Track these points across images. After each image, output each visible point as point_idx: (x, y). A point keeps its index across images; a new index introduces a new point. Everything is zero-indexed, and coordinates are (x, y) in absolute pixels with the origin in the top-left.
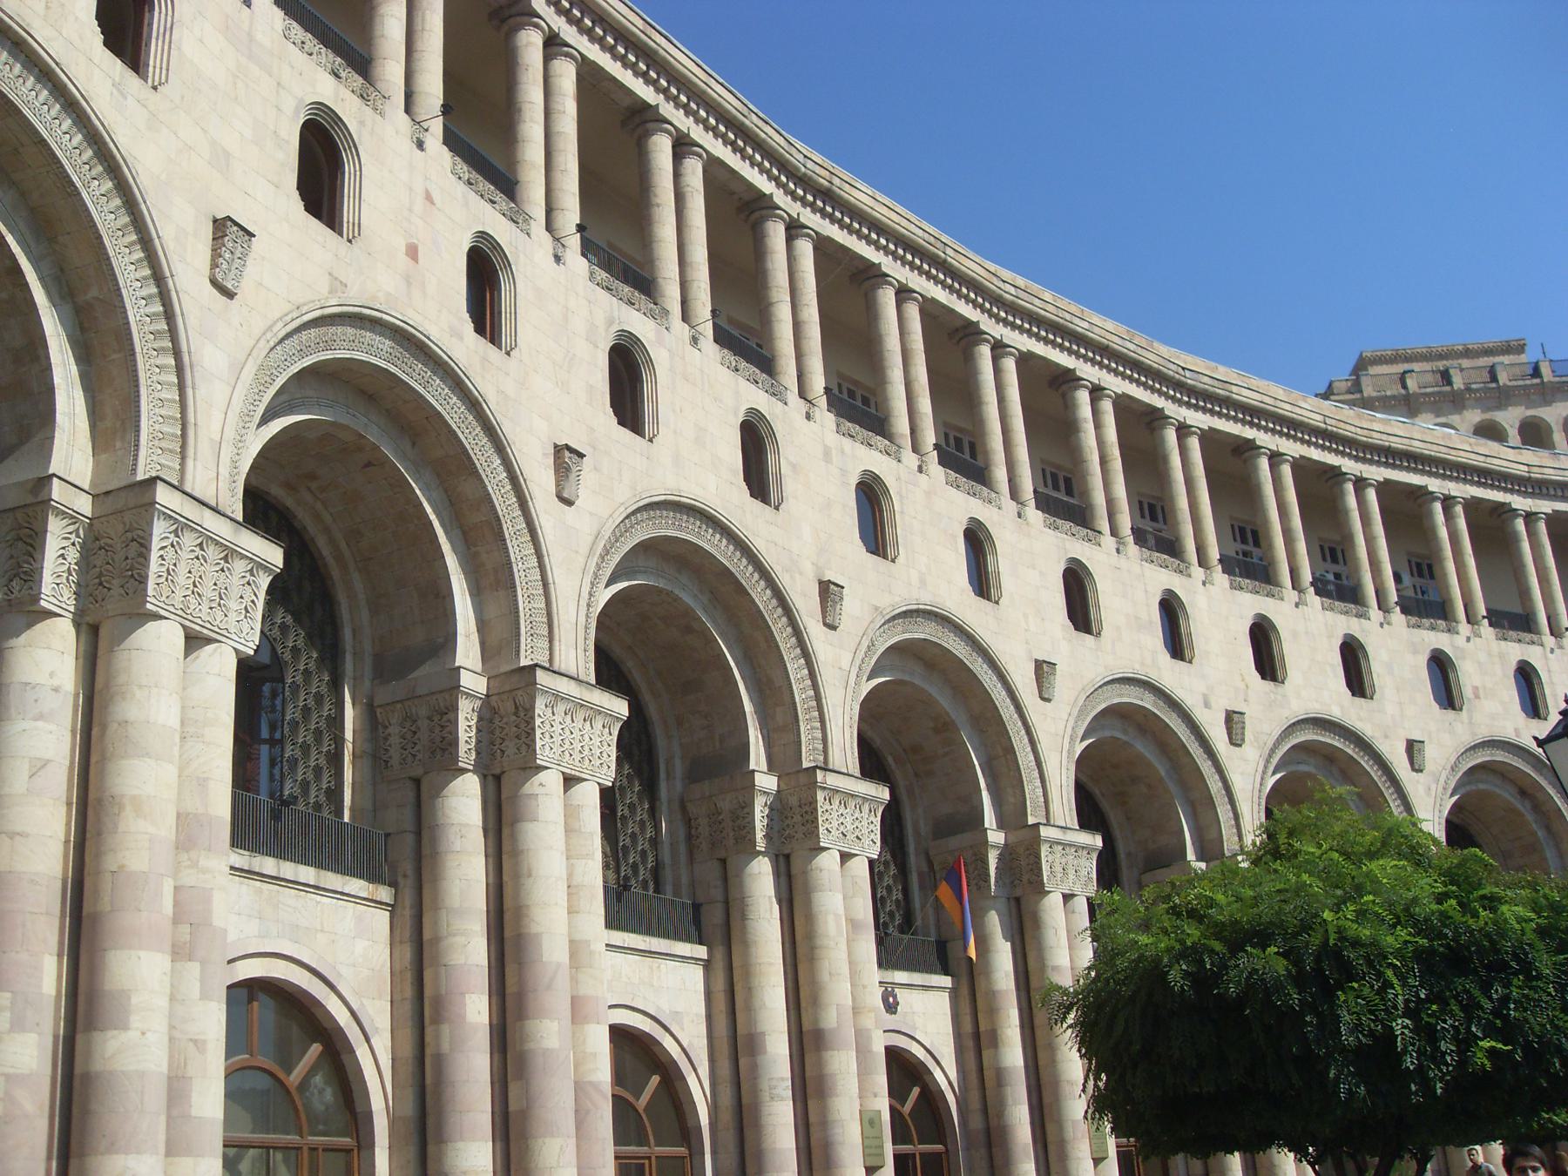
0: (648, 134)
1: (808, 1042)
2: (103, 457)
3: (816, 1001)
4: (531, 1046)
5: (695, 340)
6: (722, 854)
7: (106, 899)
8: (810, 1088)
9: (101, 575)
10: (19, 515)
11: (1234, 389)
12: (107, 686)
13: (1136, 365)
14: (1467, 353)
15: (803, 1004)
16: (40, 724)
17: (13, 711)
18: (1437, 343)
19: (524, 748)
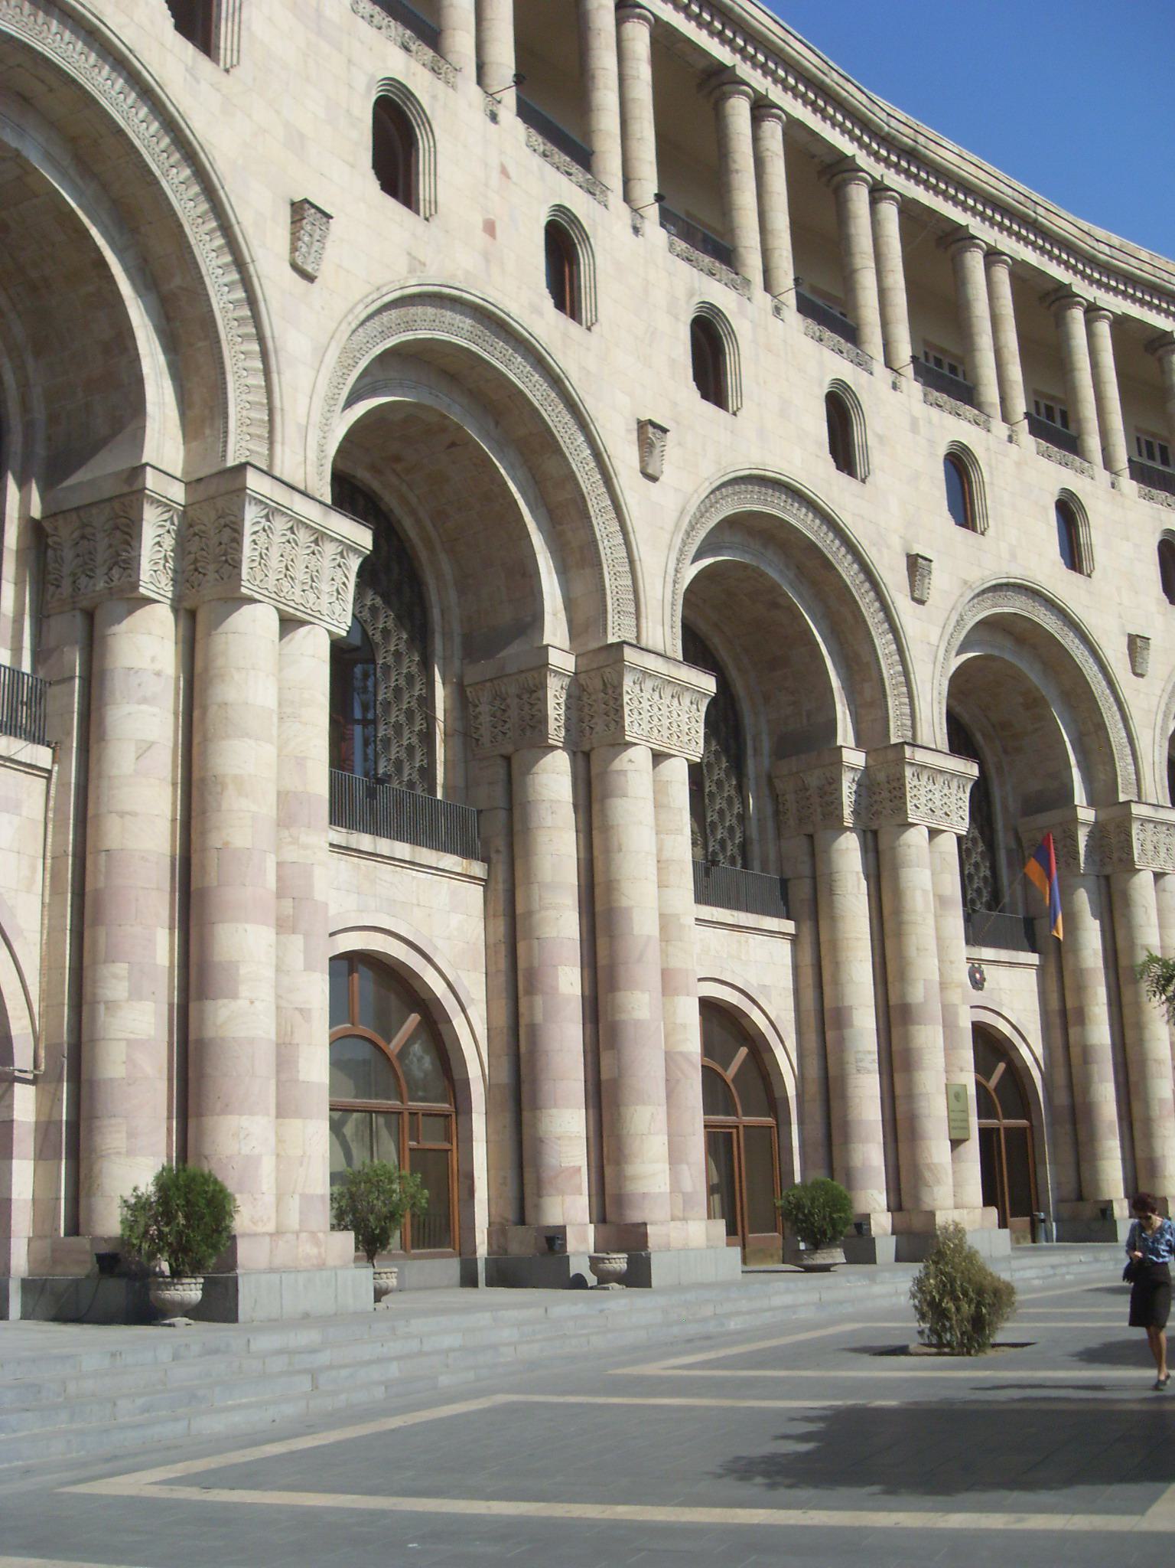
0: (724, 97)
1: (894, 1016)
2: (194, 444)
3: (903, 976)
4: (623, 1017)
5: (777, 310)
6: (810, 830)
8: (896, 1062)
9: (196, 561)
10: (116, 505)
12: (206, 669)
15: (890, 979)
16: (144, 707)
17: (118, 694)
19: (612, 725)
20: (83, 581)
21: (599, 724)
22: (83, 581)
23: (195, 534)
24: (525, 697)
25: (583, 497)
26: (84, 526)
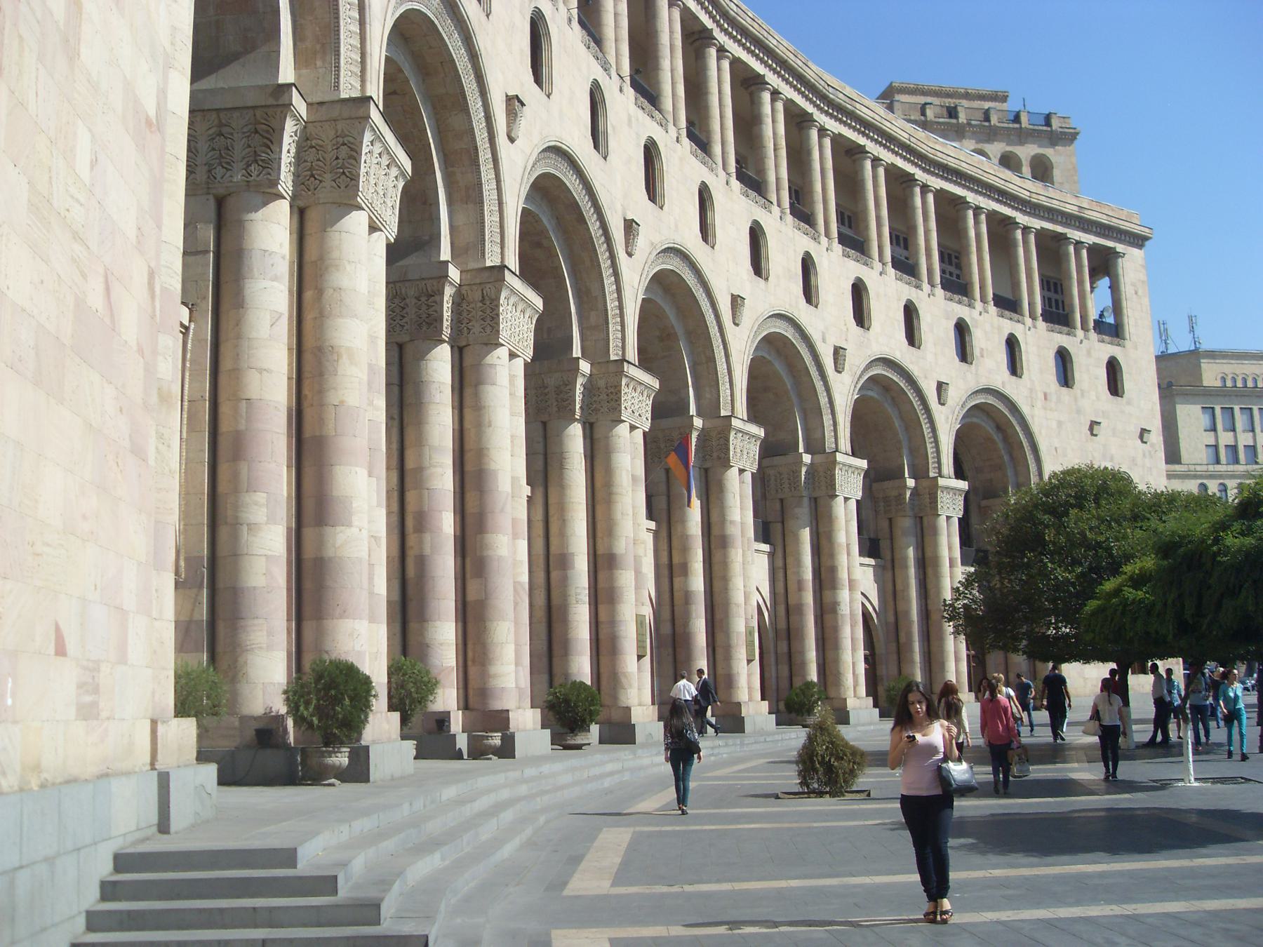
1: (603, 563)
2: (304, 71)
3: (610, 532)
4: (490, 553)
5: (570, 20)
6: (545, 418)
7: (331, 425)
8: (603, 596)
9: (311, 169)
10: (259, 113)
11: (858, 106)
12: (321, 258)
13: (800, 78)
14: (967, 96)
15: (599, 534)
16: (275, 284)
18: (947, 83)
19: (488, 330)
20: (219, 171)
21: (476, 327)
22: (219, 171)
23: (312, 147)
24: (423, 299)
25: (476, 149)
26: (221, 125)
